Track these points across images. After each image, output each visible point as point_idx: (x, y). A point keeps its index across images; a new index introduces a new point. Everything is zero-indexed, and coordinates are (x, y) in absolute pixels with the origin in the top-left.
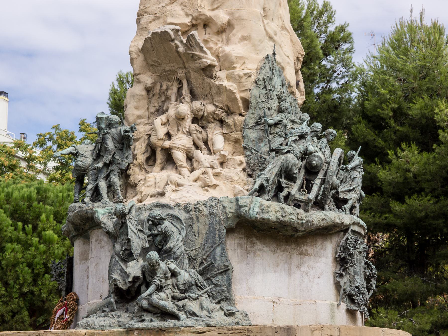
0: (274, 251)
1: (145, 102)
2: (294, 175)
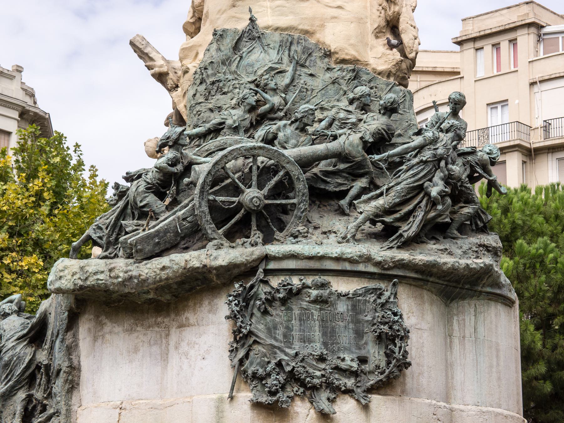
0: (131, 331)
2: (145, 209)
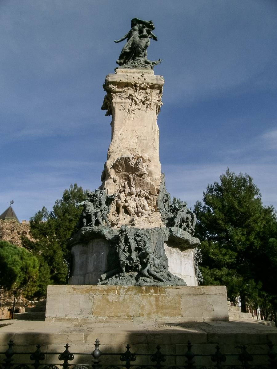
1: (114, 186)
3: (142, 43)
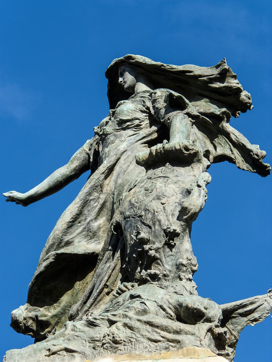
3: (158, 198)
